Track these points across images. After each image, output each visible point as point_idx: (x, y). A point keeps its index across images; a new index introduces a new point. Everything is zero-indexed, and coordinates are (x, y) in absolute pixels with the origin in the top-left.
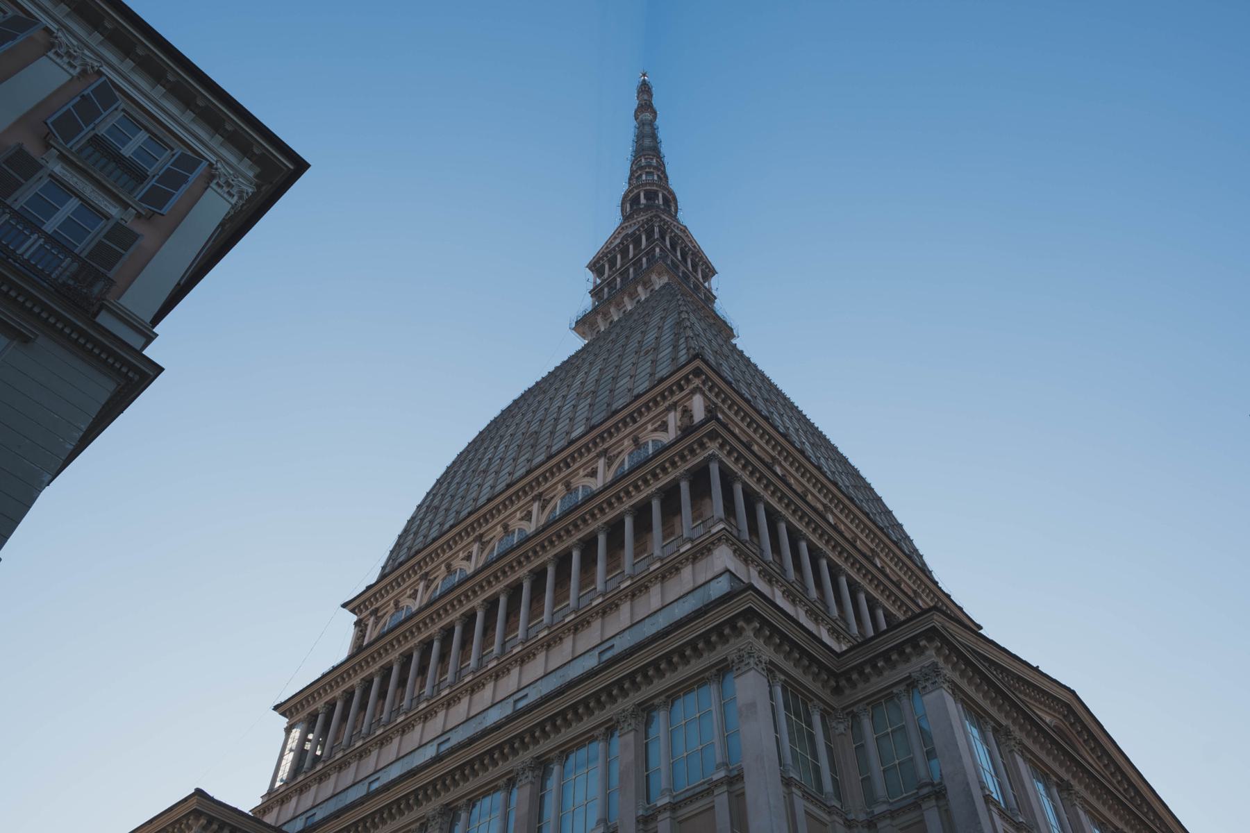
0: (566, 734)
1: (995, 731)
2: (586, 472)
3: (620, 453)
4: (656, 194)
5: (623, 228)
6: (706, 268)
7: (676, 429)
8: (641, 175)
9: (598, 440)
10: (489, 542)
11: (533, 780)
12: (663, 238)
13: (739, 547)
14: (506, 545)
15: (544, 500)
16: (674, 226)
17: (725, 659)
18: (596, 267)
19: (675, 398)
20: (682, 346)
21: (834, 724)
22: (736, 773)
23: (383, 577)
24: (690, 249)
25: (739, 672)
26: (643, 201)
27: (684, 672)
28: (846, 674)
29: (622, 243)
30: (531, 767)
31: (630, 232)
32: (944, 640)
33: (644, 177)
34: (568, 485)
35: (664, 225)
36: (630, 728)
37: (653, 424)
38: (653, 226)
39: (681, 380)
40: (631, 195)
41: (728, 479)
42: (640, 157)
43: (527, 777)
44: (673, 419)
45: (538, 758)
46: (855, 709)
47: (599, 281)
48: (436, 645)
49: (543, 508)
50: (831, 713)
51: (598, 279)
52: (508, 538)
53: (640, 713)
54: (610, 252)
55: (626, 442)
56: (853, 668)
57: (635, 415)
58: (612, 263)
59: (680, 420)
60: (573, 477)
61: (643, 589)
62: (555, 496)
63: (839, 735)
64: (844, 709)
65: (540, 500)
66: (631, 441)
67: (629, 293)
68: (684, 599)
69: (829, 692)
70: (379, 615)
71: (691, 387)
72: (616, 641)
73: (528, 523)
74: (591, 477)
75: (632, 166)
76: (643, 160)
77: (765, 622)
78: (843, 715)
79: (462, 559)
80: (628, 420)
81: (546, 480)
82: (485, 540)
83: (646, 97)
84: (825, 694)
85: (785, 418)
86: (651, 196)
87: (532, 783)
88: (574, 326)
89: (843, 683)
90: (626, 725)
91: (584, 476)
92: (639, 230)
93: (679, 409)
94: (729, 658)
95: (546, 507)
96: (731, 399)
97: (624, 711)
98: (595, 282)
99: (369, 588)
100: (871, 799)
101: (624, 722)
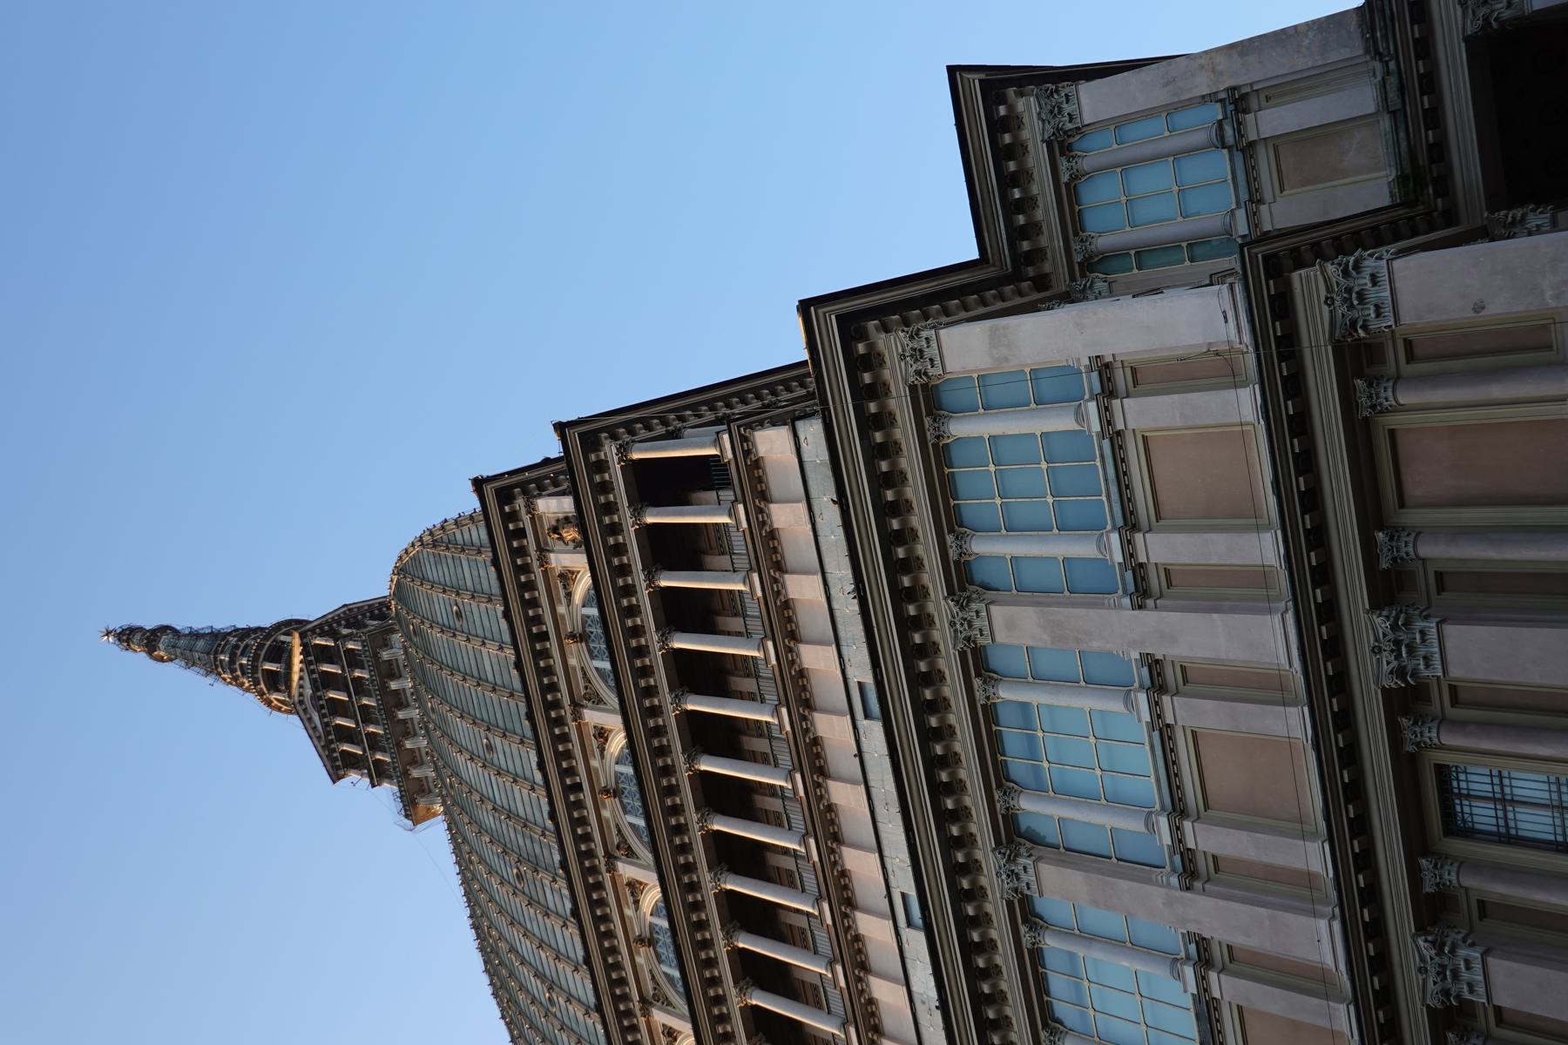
0: (970, 772)
7: (579, 553)
11: (1033, 858)
14: (668, 952)
15: (618, 847)
17: (913, 388)
18: (338, 766)
29: (319, 708)
30: (1009, 856)
31: (311, 692)
39: (506, 528)
42: (215, 659)
43: (1025, 868)
45: (998, 842)
52: (660, 943)
54: (327, 733)
58: (336, 708)
60: (598, 779)
62: (617, 825)
72: (854, 678)
81: (587, 838)
83: (138, 636)
87: (1039, 859)
95: (629, 847)
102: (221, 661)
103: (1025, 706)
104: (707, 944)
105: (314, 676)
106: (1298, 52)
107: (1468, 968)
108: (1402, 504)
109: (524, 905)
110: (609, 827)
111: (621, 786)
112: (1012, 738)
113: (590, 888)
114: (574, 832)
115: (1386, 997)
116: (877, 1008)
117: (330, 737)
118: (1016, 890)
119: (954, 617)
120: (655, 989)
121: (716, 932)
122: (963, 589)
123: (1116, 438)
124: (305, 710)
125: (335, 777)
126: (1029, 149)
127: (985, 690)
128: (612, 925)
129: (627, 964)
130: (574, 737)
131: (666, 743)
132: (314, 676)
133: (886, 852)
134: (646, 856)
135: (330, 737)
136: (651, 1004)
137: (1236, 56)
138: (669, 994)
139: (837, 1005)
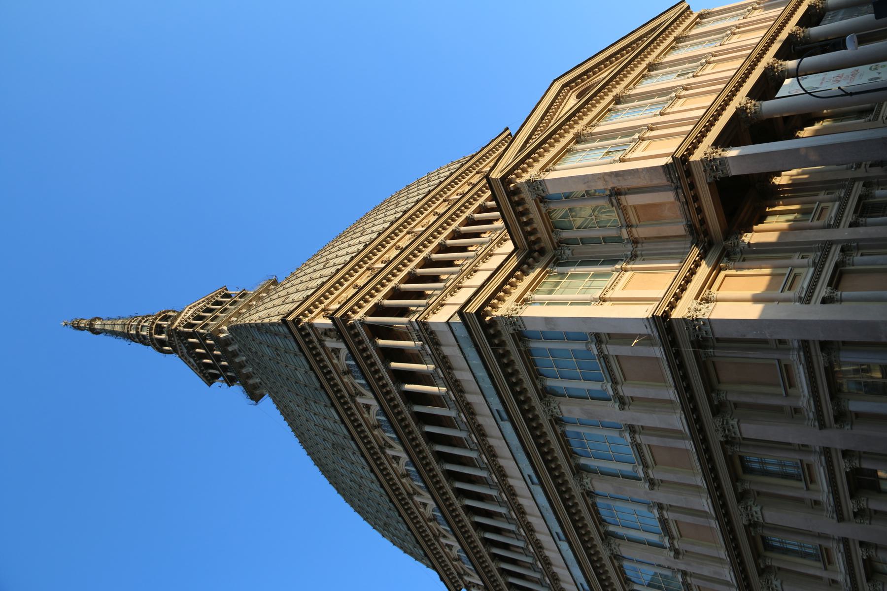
0: (559, 453)
1: (577, 142)
2: (366, 413)
3: (353, 386)
4: (159, 326)
5: (183, 356)
6: (220, 294)
8: (143, 336)
9: (342, 401)
10: (414, 489)
11: (589, 479)
12: (192, 326)
13: (431, 310)
15: (385, 445)
16: (185, 316)
17: (512, 335)
18: (210, 380)
19: (315, 340)
20: (276, 328)
21: (565, 257)
22: (594, 338)
23: (434, 568)
24: (205, 306)
25: (522, 326)
26: (163, 336)
27: (520, 365)
28: (531, 244)
29: (193, 358)
30: (580, 480)
31: (186, 351)
32: (511, 172)
33: (145, 333)
34: (375, 426)
35: (183, 323)
36: (557, 408)
37: (334, 359)
38: (183, 332)
40: (158, 346)
41: (378, 310)
43: (587, 484)
44: (331, 343)
46: (555, 241)
47: (221, 379)
48: (488, 536)
49: (391, 447)
50: (557, 258)
51: (220, 379)
53: (547, 399)
54: (200, 367)
55: (346, 380)
56: (526, 239)
57: (325, 371)
59: (332, 338)
60: (369, 422)
61: (457, 384)
63: (573, 255)
64: (555, 249)
65: (384, 448)
66: (345, 376)
67: (233, 357)
68: (467, 355)
69: (542, 258)
70: (463, 573)
71: (307, 327)
72: (494, 408)
73: (401, 458)
74: (370, 408)
75: (136, 342)
76: (131, 332)
77: (487, 303)
78: (559, 249)
79: (425, 509)
80: (328, 377)
81: (370, 442)
82: (412, 492)
84: (545, 260)
85: (340, 253)
86: (160, 330)
88: (254, 402)
89: (536, 247)
90: (555, 410)
91: (369, 414)
92: (185, 343)
93: (323, 338)
94: (511, 332)
96: (320, 297)
97: (544, 411)
98: (222, 381)
99: (442, 579)
100: (619, 240)
101: (552, 411)
102: (132, 334)
103: (578, 434)
104: (365, 350)
105: (186, 345)
106: (640, 178)
107: (733, 427)
108: (719, 382)
109: (340, 460)
110: (378, 438)
111: (380, 423)
112: (573, 442)
113: (346, 410)
114: (363, 442)
115: (705, 440)
116: (482, 427)
117: (202, 369)
118: (584, 490)
119: (544, 408)
120: (355, 390)
121: (434, 464)
122: (545, 397)
123: (606, 358)
124: (186, 358)
125: (210, 383)
126: (526, 200)
127: (561, 429)
128: (325, 363)
129: (339, 382)
130: (373, 440)
131: (373, 361)
132: (186, 345)
133: (507, 440)
134: (371, 395)
135: (202, 369)
136: (355, 396)
137: (613, 176)
138: (361, 390)
139: (463, 426)
